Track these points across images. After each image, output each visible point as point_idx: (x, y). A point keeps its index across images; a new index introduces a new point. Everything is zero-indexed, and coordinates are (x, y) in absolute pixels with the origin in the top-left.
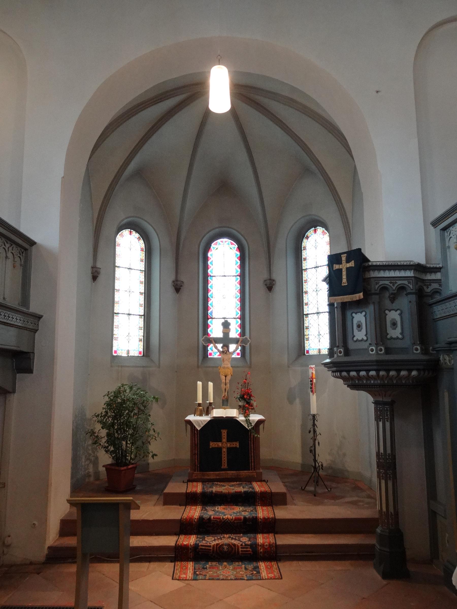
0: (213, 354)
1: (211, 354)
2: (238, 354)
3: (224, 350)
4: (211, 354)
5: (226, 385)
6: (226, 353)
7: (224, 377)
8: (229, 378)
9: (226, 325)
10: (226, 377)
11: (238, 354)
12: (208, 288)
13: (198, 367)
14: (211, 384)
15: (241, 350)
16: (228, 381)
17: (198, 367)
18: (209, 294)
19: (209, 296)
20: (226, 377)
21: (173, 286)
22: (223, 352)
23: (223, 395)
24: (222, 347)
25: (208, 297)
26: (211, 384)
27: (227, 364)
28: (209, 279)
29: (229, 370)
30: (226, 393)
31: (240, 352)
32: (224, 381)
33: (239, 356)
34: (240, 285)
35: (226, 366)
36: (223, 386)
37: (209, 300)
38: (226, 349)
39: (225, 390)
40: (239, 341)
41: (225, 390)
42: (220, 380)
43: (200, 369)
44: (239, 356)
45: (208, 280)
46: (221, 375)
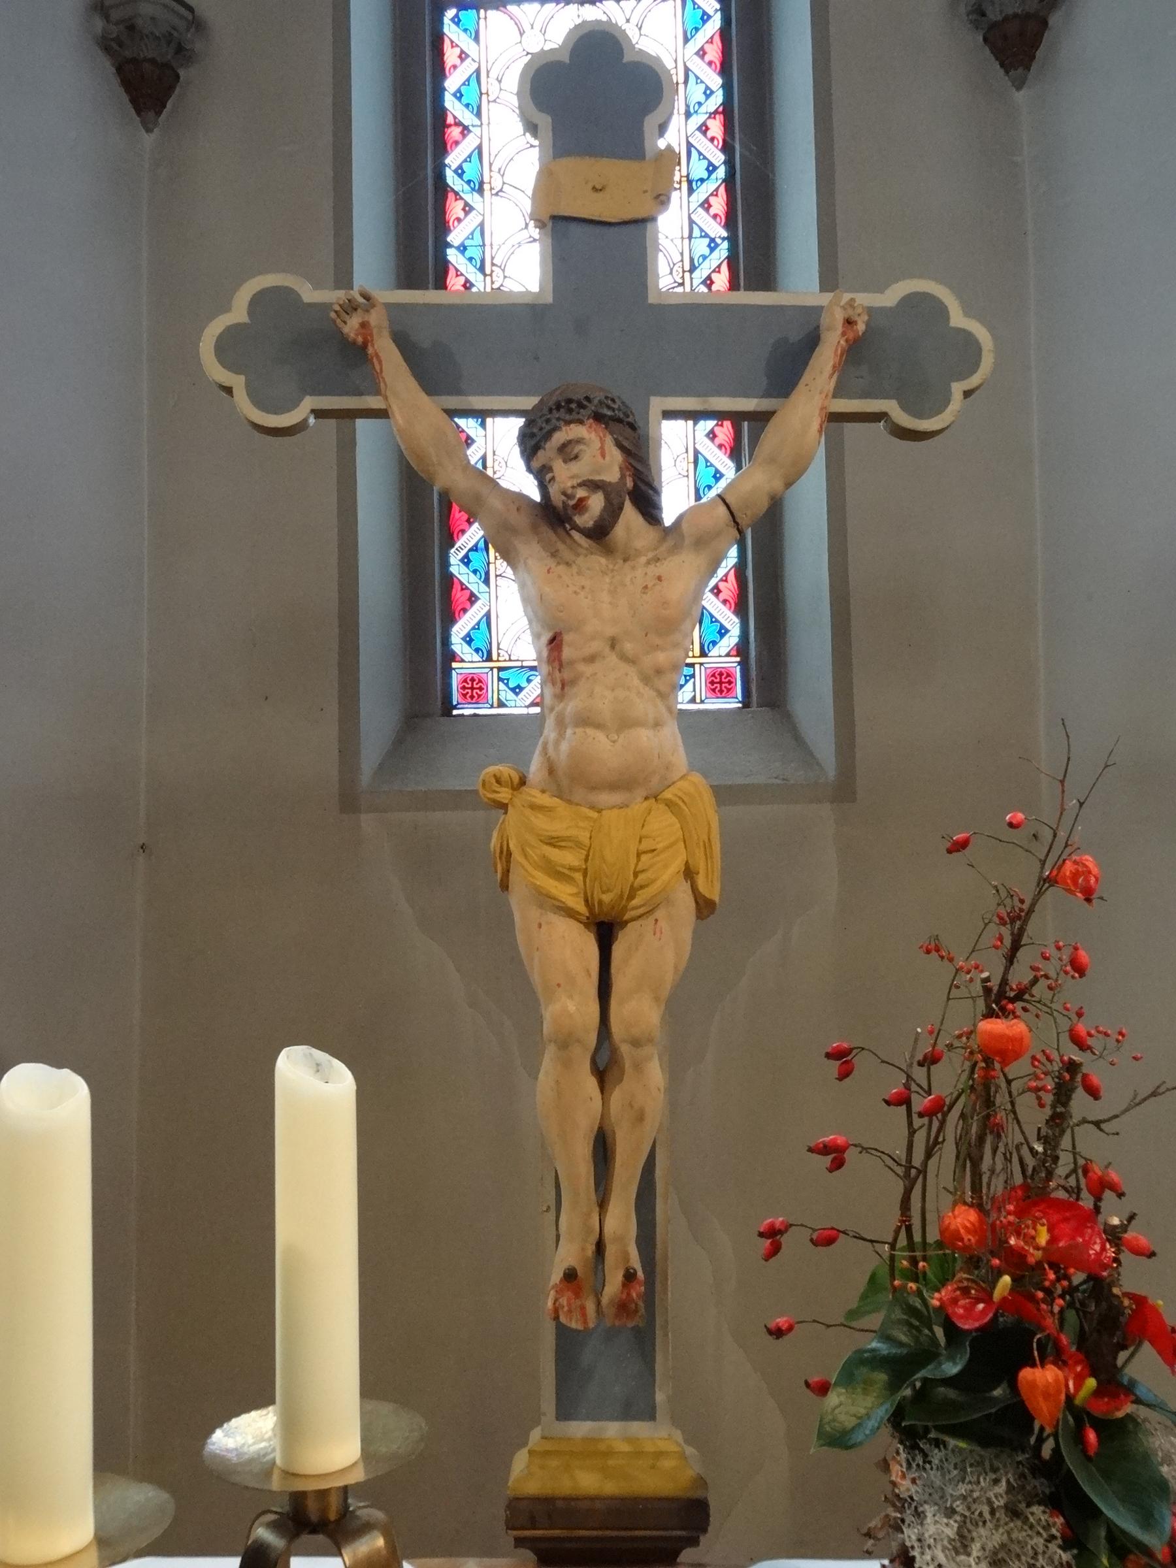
0: (495, 690)
1: (474, 688)
2: (719, 683)
3: (565, 475)
4: (474, 688)
5: (606, 1070)
6: (600, 533)
7: (574, 948)
8: (657, 951)
9: (593, 98)
10: (606, 931)
11: (719, 683)
12: (440, 113)
13: (349, 800)
14: (315, 1095)
15: (741, 650)
16: (638, 1011)
17: (349, 800)
18: (453, 159)
19: (451, 178)
20: (606, 931)
21: (107, 45)
22: (553, 516)
23: (569, 1254)
24: (531, 444)
25: (442, 190)
26: (315, 1095)
27: (626, 723)
28: (450, 30)
29: (663, 824)
30: (620, 1220)
31: (733, 663)
32: (574, 1007)
33: (731, 704)
34: (724, 70)
35: (606, 749)
36: (562, 1099)
37: (455, 209)
38: (597, 455)
39: (603, 1149)
40: (812, 341)
41: (603, 1149)
42: (512, 986)
43: (368, 822)
44: (731, 704)
45: (438, 39)
46: (517, 899)
